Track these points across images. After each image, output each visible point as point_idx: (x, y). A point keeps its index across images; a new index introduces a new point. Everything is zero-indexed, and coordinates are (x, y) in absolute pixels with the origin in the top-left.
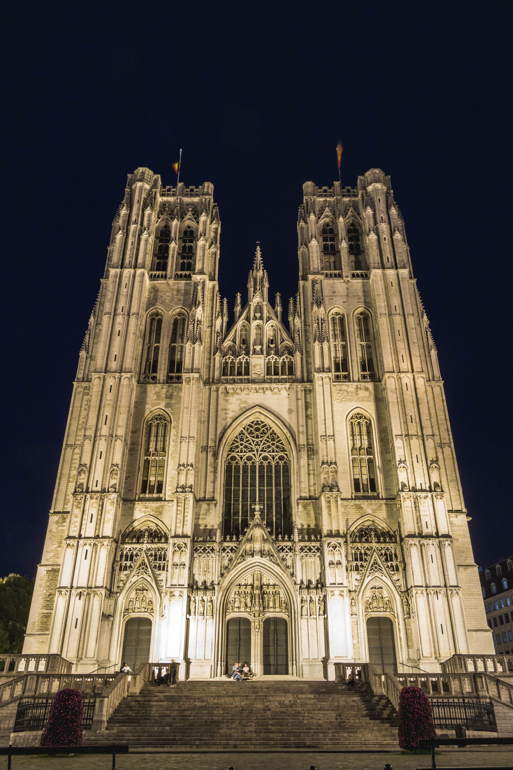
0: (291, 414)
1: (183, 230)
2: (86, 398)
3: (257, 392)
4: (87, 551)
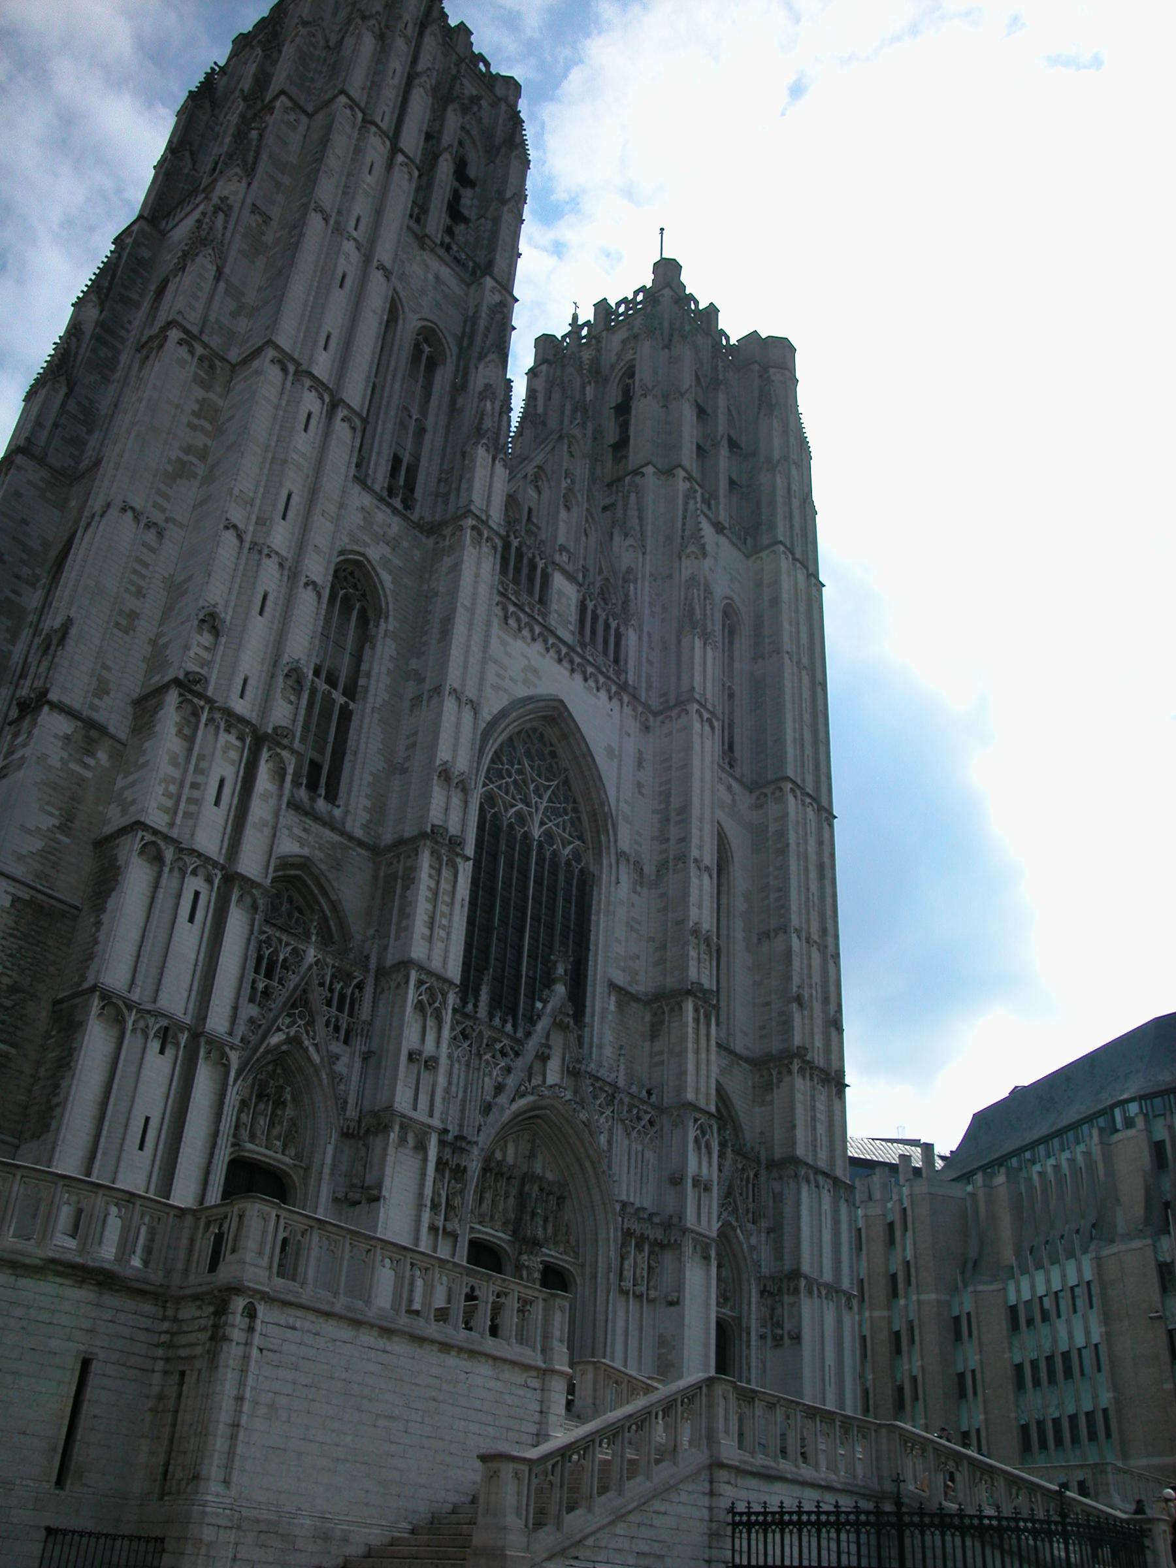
2: (200, 393)
3: (560, 661)
4: (197, 894)
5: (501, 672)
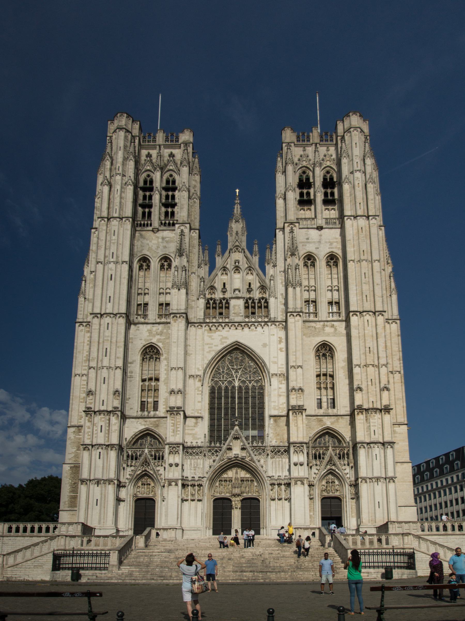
0: (266, 347)
1: (165, 178)
3: (236, 329)
4: (100, 452)
5: (211, 346)
